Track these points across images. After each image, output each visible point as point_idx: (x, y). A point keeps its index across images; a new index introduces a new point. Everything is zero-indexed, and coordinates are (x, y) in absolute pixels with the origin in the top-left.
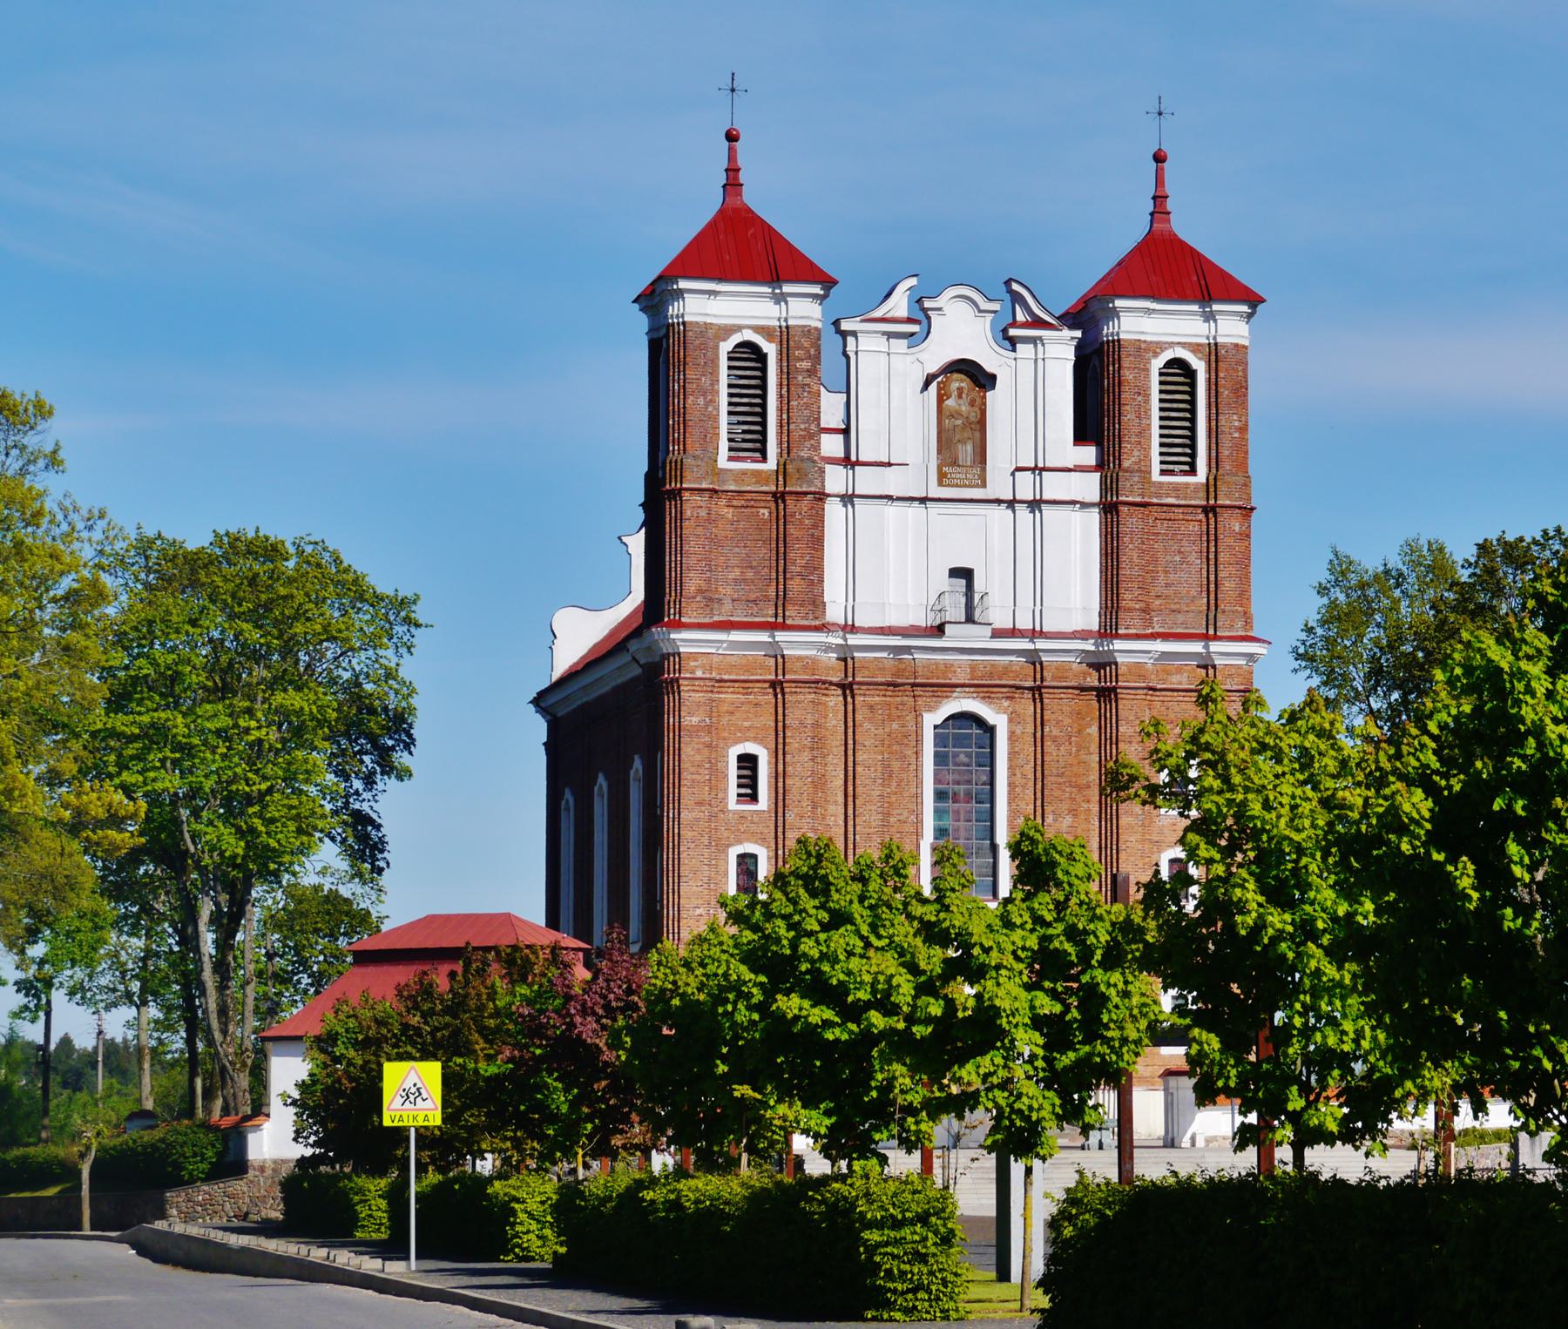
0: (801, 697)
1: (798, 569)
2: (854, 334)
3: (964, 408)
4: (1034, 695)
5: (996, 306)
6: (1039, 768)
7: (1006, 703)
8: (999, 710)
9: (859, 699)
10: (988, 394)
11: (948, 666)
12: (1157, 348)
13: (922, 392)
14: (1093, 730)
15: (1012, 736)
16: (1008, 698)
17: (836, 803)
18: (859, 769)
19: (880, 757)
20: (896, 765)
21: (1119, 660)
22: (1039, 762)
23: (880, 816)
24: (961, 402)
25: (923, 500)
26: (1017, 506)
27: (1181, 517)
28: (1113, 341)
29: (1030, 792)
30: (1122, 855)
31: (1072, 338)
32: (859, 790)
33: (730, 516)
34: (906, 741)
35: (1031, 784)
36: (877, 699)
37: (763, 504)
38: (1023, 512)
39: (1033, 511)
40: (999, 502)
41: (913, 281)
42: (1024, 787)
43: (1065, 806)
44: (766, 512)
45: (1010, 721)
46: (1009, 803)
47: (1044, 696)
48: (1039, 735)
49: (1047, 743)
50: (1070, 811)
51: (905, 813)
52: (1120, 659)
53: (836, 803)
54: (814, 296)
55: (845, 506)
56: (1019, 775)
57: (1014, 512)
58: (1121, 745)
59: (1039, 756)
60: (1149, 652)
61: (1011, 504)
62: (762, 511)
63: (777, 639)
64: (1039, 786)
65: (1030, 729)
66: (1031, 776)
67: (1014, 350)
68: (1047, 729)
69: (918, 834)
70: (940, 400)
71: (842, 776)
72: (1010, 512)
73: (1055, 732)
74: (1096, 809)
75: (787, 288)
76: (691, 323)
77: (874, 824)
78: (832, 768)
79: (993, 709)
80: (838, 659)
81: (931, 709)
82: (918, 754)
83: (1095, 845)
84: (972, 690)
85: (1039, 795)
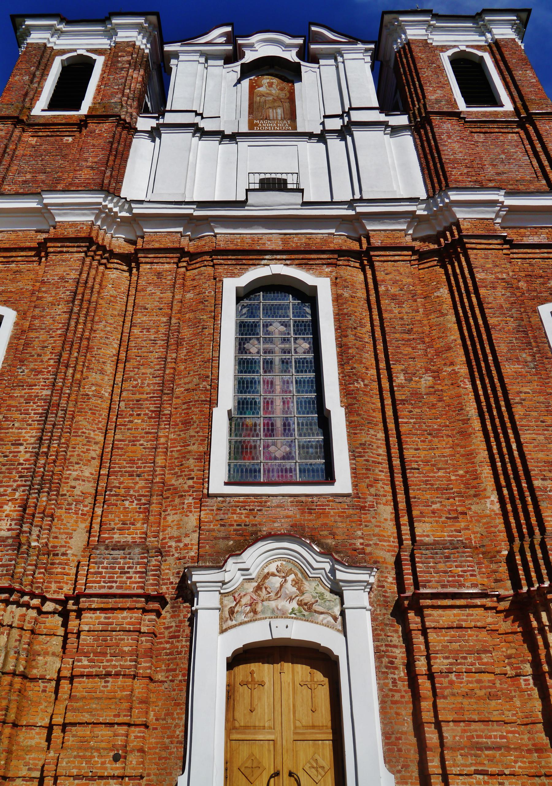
0: (67, 256)
1: (89, 164)
2: (176, 55)
3: (274, 92)
4: (362, 264)
5: (300, 41)
6: (378, 329)
7: (328, 269)
8: (320, 275)
9: (144, 268)
10: (297, 85)
11: (256, 238)
12: (444, 48)
13: (235, 85)
14: (444, 292)
15: (337, 299)
16: (328, 264)
17: (102, 372)
18: (136, 331)
19: (164, 319)
20: (186, 332)
21: (459, 216)
22: (377, 323)
23: (157, 380)
24: (271, 89)
25: (233, 137)
26: (328, 136)
27: (497, 130)
28: (404, 48)
29: (369, 357)
30: (518, 411)
31: (367, 50)
32: (133, 352)
33: (34, 142)
34: (201, 306)
35: (370, 347)
36: (167, 266)
37: (67, 134)
38: (335, 144)
39: (344, 139)
40: (310, 136)
41: (229, 29)
42: (361, 349)
43: (420, 364)
44: (70, 139)
45: (334, 284)
46: (341, 364)
47: (374, 258)
48: (373, 298)
49: (384, 302)
50: (427, 370)
51: (196, 380)
52: (461, 214)
53: (102, 372)
54: (139, 26)
55: (154, 141)
56: (351, 337)
57: (325, 143)
58: (482, 291)
59: (376, 317)
60: (492, 203)
61: (322, 137)
62: (66, 138)
63: (45, 201)
64: (380, 347)
65: (361, 294)
66: (368, 338)
67: (318, 63)
68: (382, 289)
69: (213, 402)
70: (252, 88)
71: (116, 346)
72: (322, 146)
73: (393, 290)
74: (464, 370)
75: (116, 21)
76: (32, 44)
77: (147, 389)
78: (102, 334)
79: (313, 274)
80: (126, 240)
81: (233, 275)
82: (216, 316)
83: (472, 409)
84: (284, 257)
85: (381, 356)
